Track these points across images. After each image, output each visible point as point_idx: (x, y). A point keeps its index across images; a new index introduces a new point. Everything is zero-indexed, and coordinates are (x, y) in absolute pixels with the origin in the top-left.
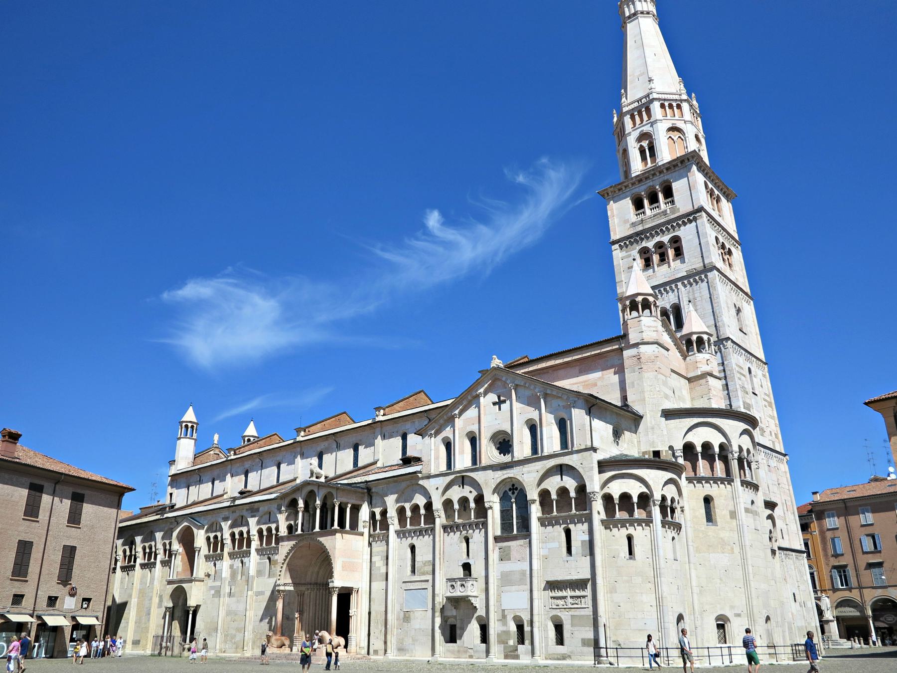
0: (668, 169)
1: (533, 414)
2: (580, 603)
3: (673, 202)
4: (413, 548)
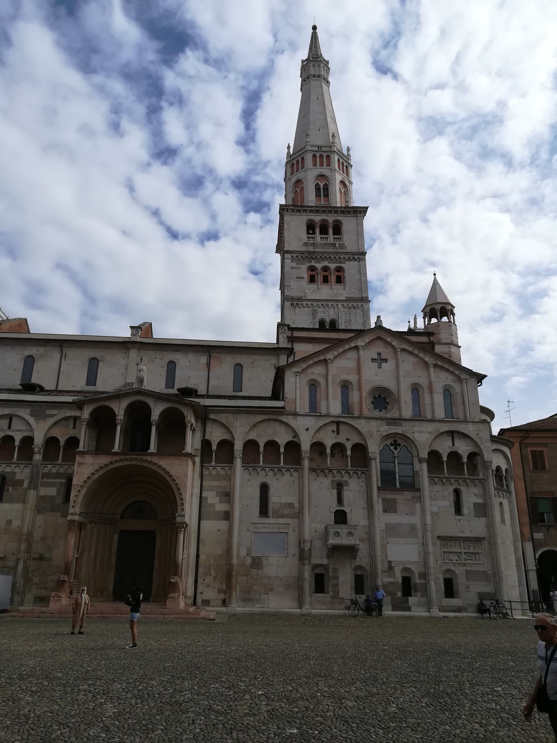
1: (423, 381)
2: (474, 559)
4: (264, 489)
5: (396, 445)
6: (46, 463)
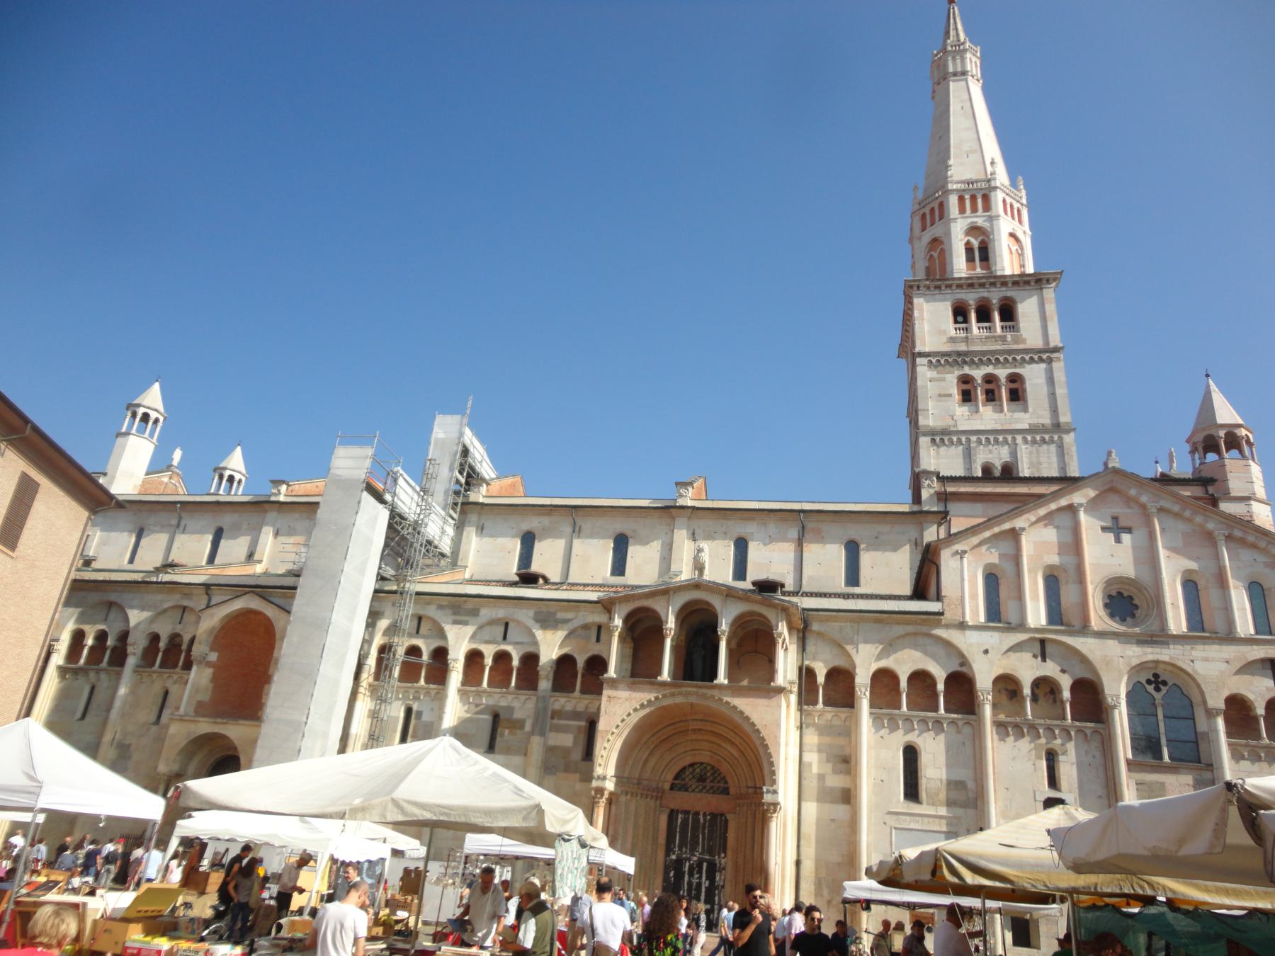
0: (1016, 283)
3: (1014, 329)
4: (911, 755)
6: (557, 694)
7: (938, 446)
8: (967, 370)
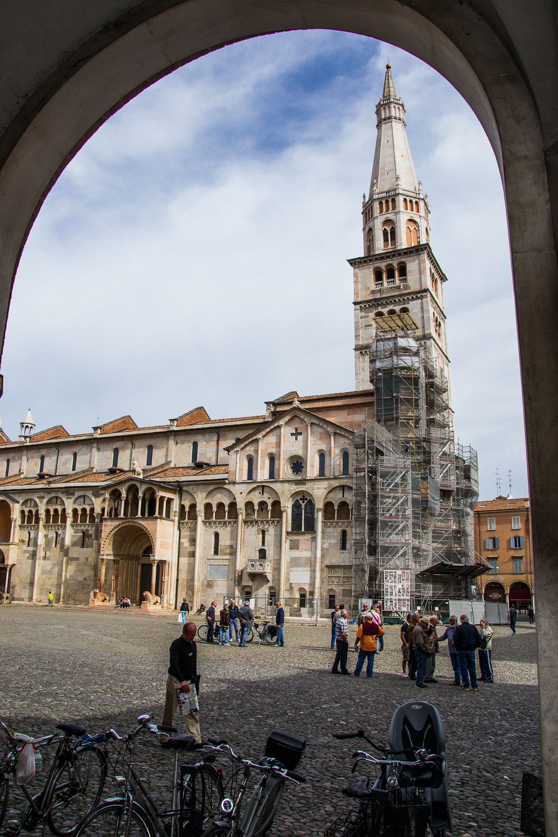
4: (217, 535)
5: (303, 499)
7: (364, 355)
8: (380, 309)
